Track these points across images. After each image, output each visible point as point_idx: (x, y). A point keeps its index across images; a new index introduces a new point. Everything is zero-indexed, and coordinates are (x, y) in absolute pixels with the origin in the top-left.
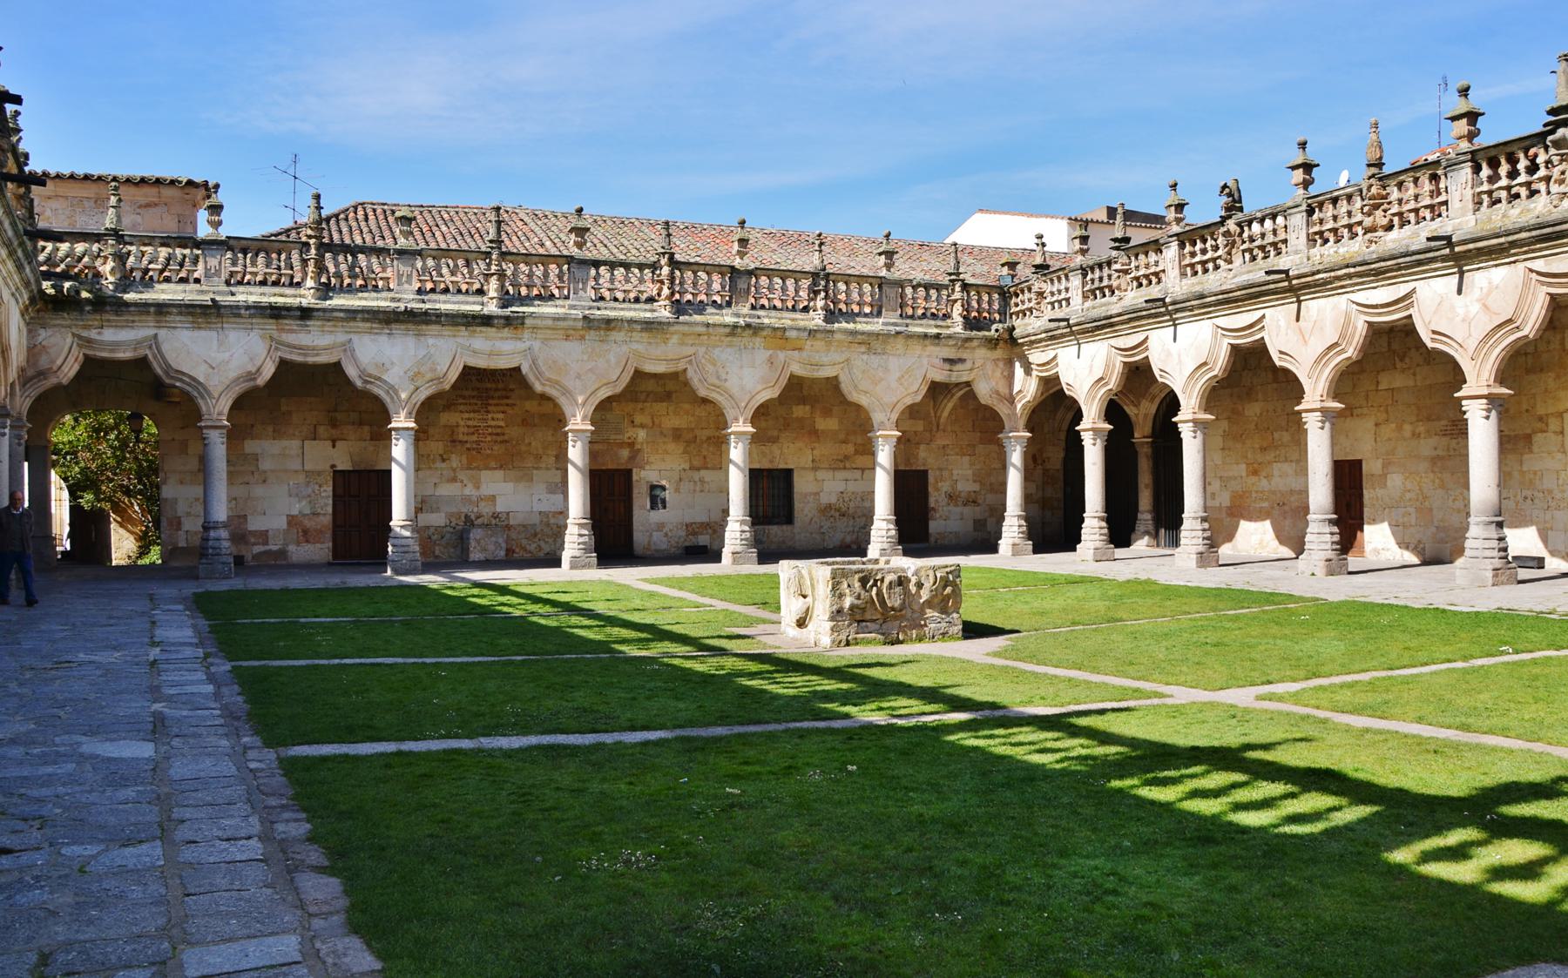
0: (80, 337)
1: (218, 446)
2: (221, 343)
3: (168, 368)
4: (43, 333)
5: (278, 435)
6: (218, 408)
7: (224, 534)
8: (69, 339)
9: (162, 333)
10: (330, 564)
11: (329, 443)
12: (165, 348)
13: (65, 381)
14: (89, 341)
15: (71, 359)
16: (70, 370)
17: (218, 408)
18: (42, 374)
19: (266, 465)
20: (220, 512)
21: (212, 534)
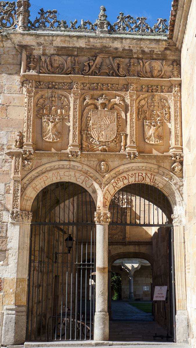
7: (133, 294)
9: (123, 261)
10: (151, 301)
11: (150, 278)
20: (132, 291)
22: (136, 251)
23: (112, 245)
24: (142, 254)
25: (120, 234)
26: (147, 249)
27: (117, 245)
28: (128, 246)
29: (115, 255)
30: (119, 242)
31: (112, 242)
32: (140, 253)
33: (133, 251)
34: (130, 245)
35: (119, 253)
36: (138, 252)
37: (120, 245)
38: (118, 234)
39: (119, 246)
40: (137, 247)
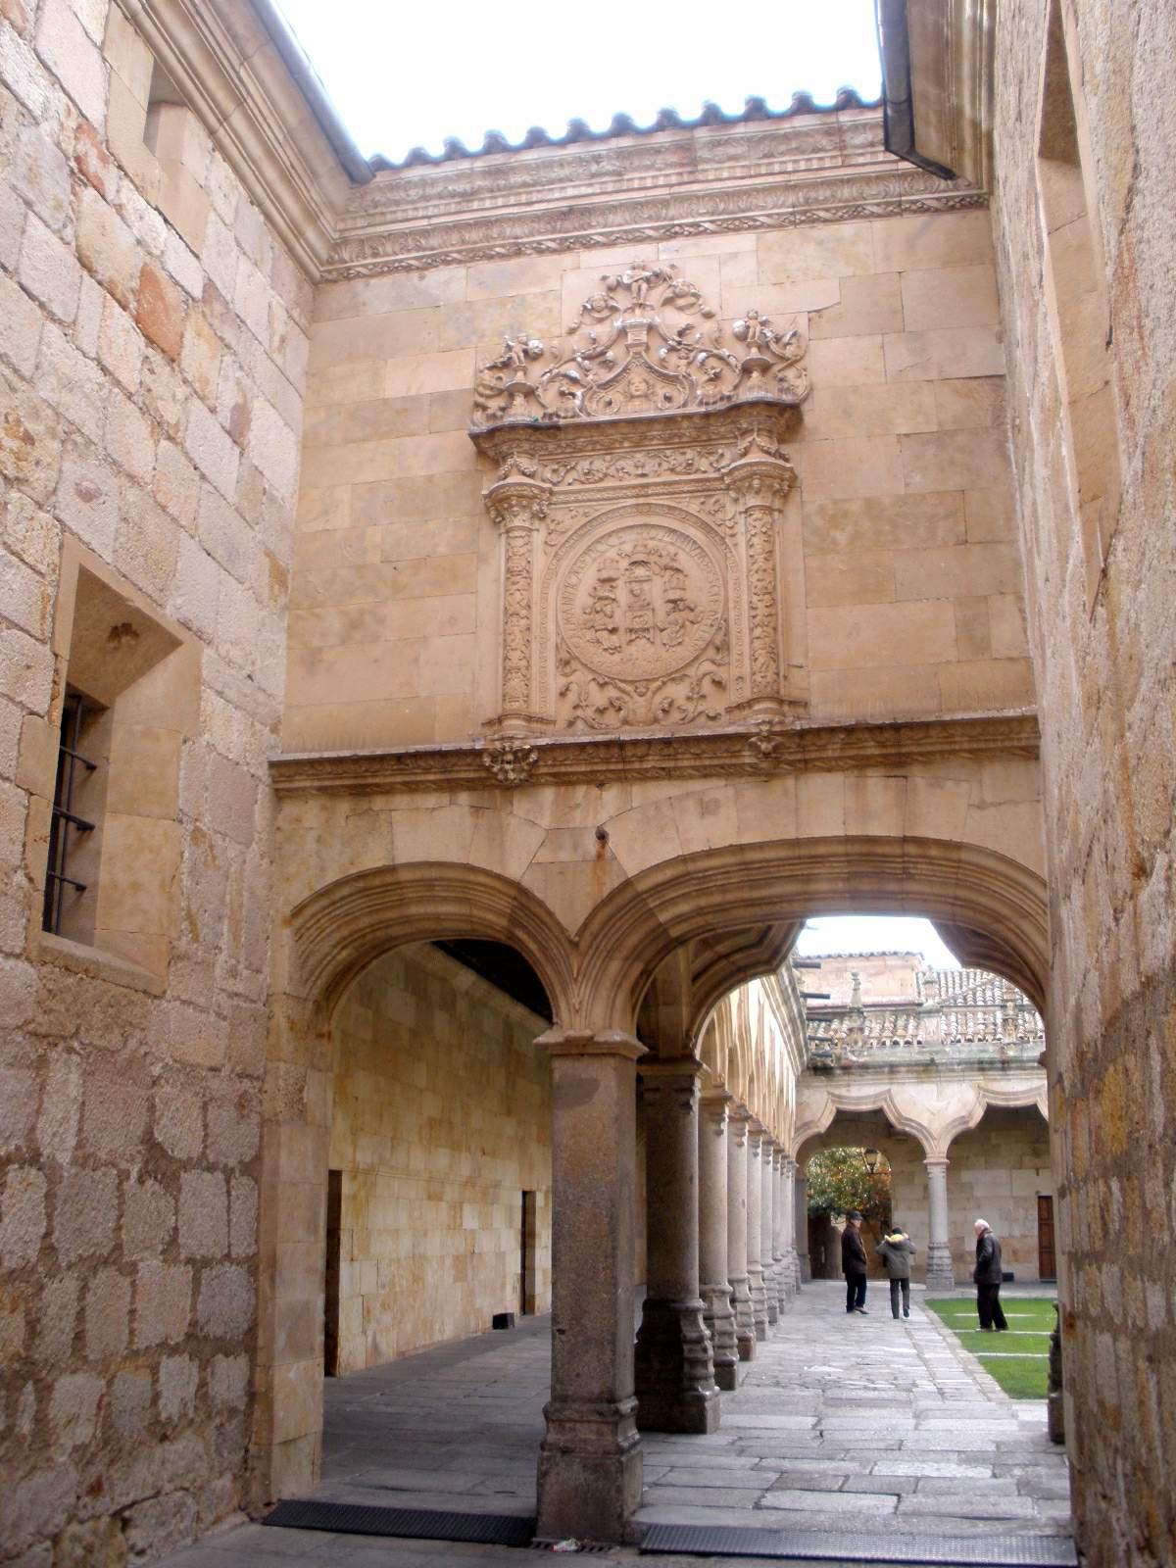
0: (833, 1095)
1: (938, 1177)
2: (939, 1093)
3: (900, 1117)
4: (806, 1092)
5: (988, 1165)
6: (937, 1150)
7: (946, 1253)
8: (825, 1096)
9: (894, 1088)
12: (896, 1100)
13: (823, 1130)
14: (839, 1097)
15: (827, 1113)
16: (825, 1122)
17: (937, 1150)
18: (806, 1125)
19: (979, 1192)
21: (936, 1253)
22: (876, 829)
23: (623, 778)
24: (934, 852)
25: (707, 667)
26: (981, 806)
27: (669, 774)
28: (790, 782)
29: (660, 877)
30: (686, 740)
31: (621, 745)
32: (912, 849)
33: (841, 833)
34: (804, 767)
35: (693, 857)
36: (894, 832)
37: (705, 773)
38: (691, 671)
39: (696, 785)
40: (878, 788)
